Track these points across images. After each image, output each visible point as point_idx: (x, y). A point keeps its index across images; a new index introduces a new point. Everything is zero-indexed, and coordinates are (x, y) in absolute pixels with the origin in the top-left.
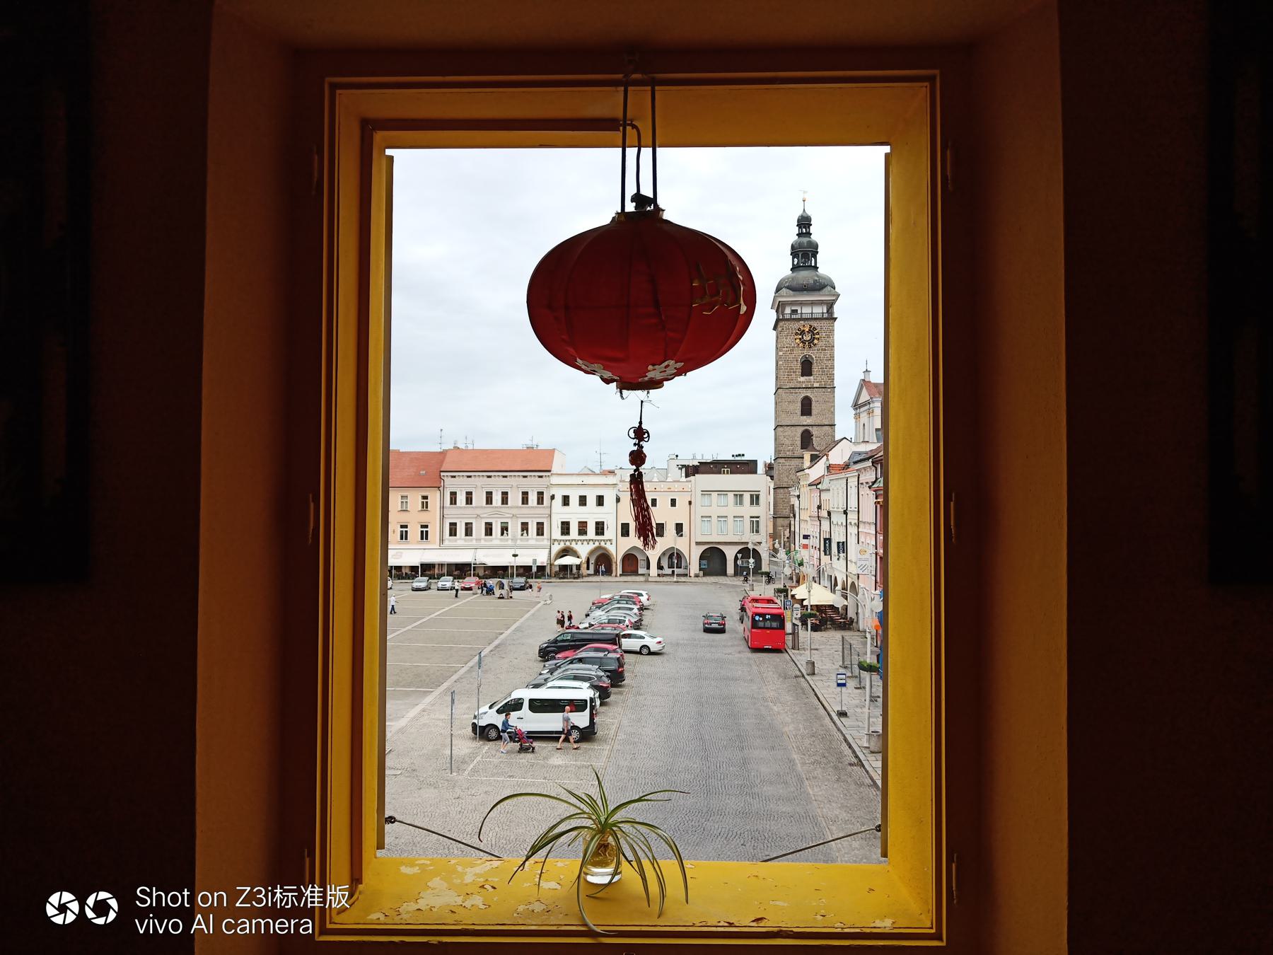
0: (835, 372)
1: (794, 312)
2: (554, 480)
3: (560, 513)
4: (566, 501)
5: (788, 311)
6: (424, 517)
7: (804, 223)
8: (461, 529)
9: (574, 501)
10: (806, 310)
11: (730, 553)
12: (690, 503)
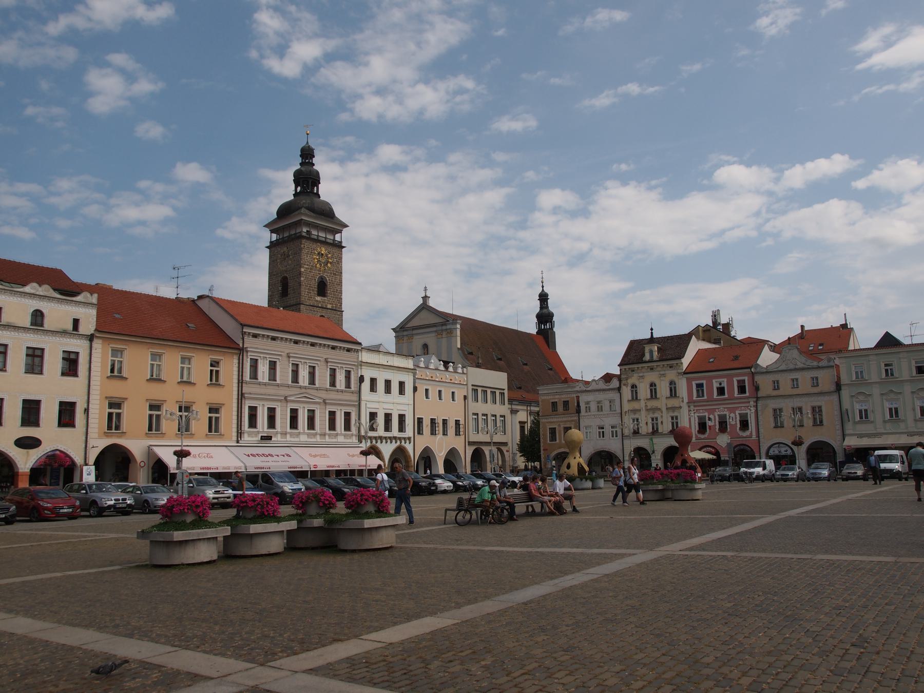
0: (343, 297)
5: (305, 230)
6: (215, 395)
7: (307, 154)
9: (381, 386)
10: (322, 234)
12: (465, 397)
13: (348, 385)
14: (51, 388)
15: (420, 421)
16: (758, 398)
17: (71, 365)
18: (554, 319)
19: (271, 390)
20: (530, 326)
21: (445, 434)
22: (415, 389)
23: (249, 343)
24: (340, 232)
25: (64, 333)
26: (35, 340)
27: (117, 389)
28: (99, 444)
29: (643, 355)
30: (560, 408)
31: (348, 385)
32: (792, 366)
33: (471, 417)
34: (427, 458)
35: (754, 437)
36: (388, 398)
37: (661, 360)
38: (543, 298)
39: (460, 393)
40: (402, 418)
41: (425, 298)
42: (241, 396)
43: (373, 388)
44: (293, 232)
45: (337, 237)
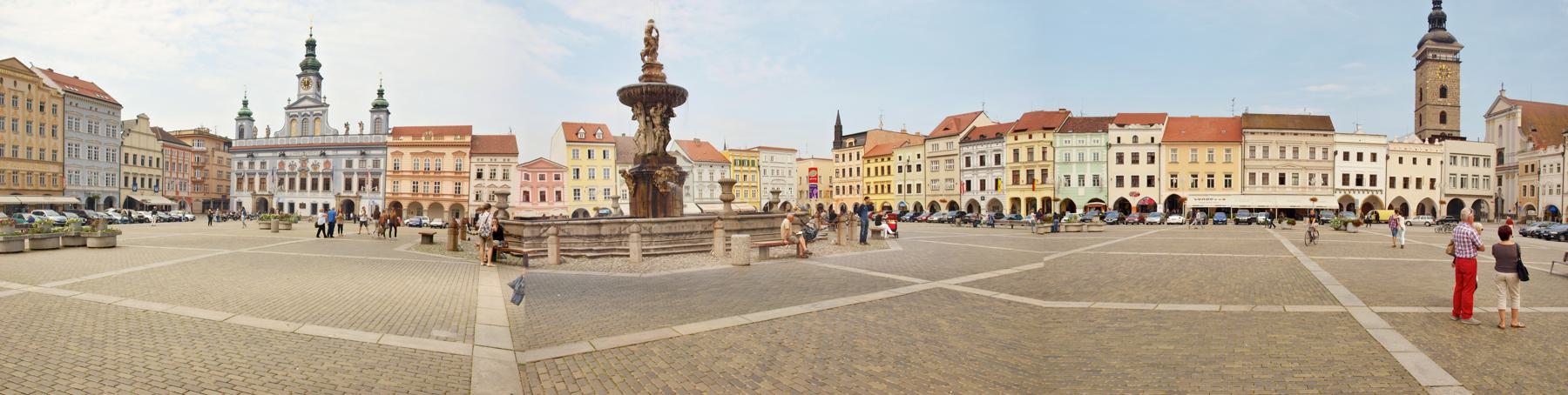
2: (1338, 138)
4: (1346, 156)
6: (1228, 169)
8: (1259, 178)
9: (1353, 156)
11: (1468, 203)
13: (1325, 158)
14: (1143, 169)
17: (1152, 159)
19: (1268, 163)
26: (1134, 149)
27: (1174, 169)
28: (1166, 194)
31: (1325, 158)
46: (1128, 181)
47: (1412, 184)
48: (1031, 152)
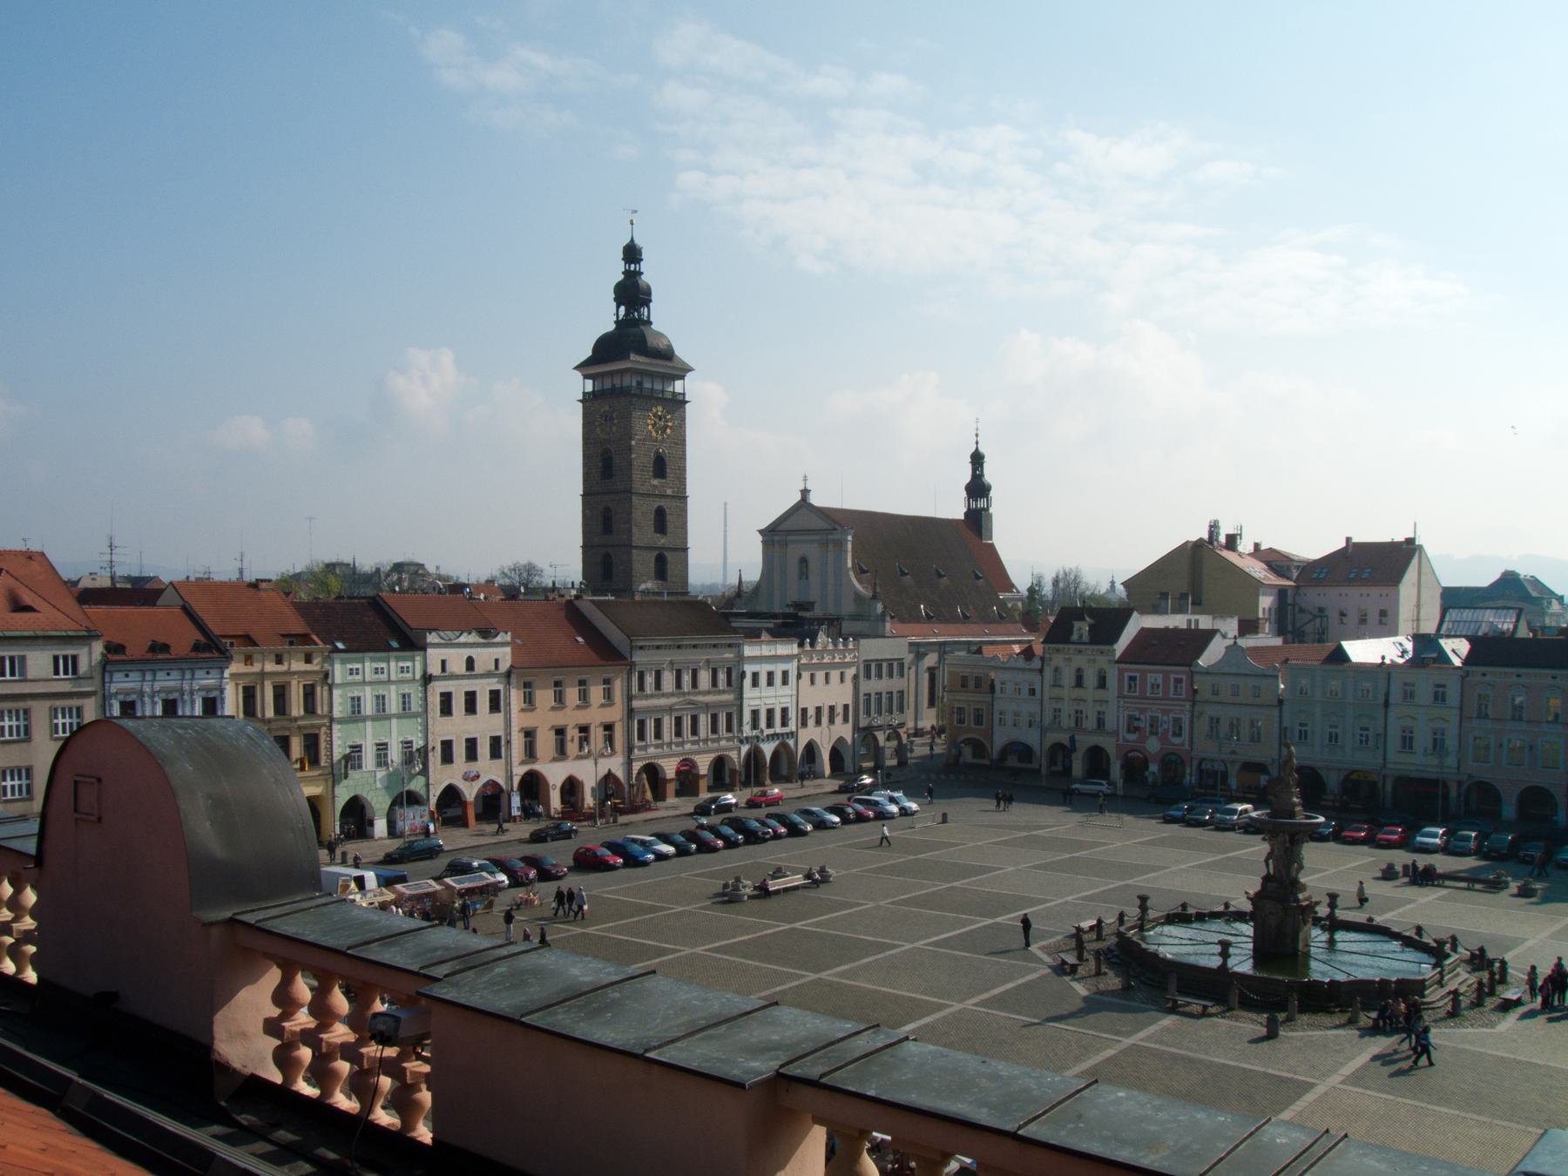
1: (640, 384)
2: (748, 651)
3: (755, 698)
9: (763, 680)
14: (485, 725)
15: (804, 711)
16: (1194, 703)
17: (495, 702)
18: (992, 494)
20: (954, 508)
21: (832, 721)
22: (799, 676)
23: (638, 657)
24: (682, 378)
25: (488, 675)
26: (468, 685)
28: (519, 771)
29: (1071, 633)
30: (971, 684)
31: (729, 683)
32: (1234, 670)
33: (862, 698)
34: (811, 749)
35: (1187, 746)
36: (770, 691)
37: (1092, 642)
38: (977, 459)
39: (850, 673)
40: (785, 711)
41: (805, 492)
42: (631, 712)
43: (755, 683)
44: (617, 382)
45: (678, 386)
46: (459, 751)
47: (825, 719)
48: (281, 694)
